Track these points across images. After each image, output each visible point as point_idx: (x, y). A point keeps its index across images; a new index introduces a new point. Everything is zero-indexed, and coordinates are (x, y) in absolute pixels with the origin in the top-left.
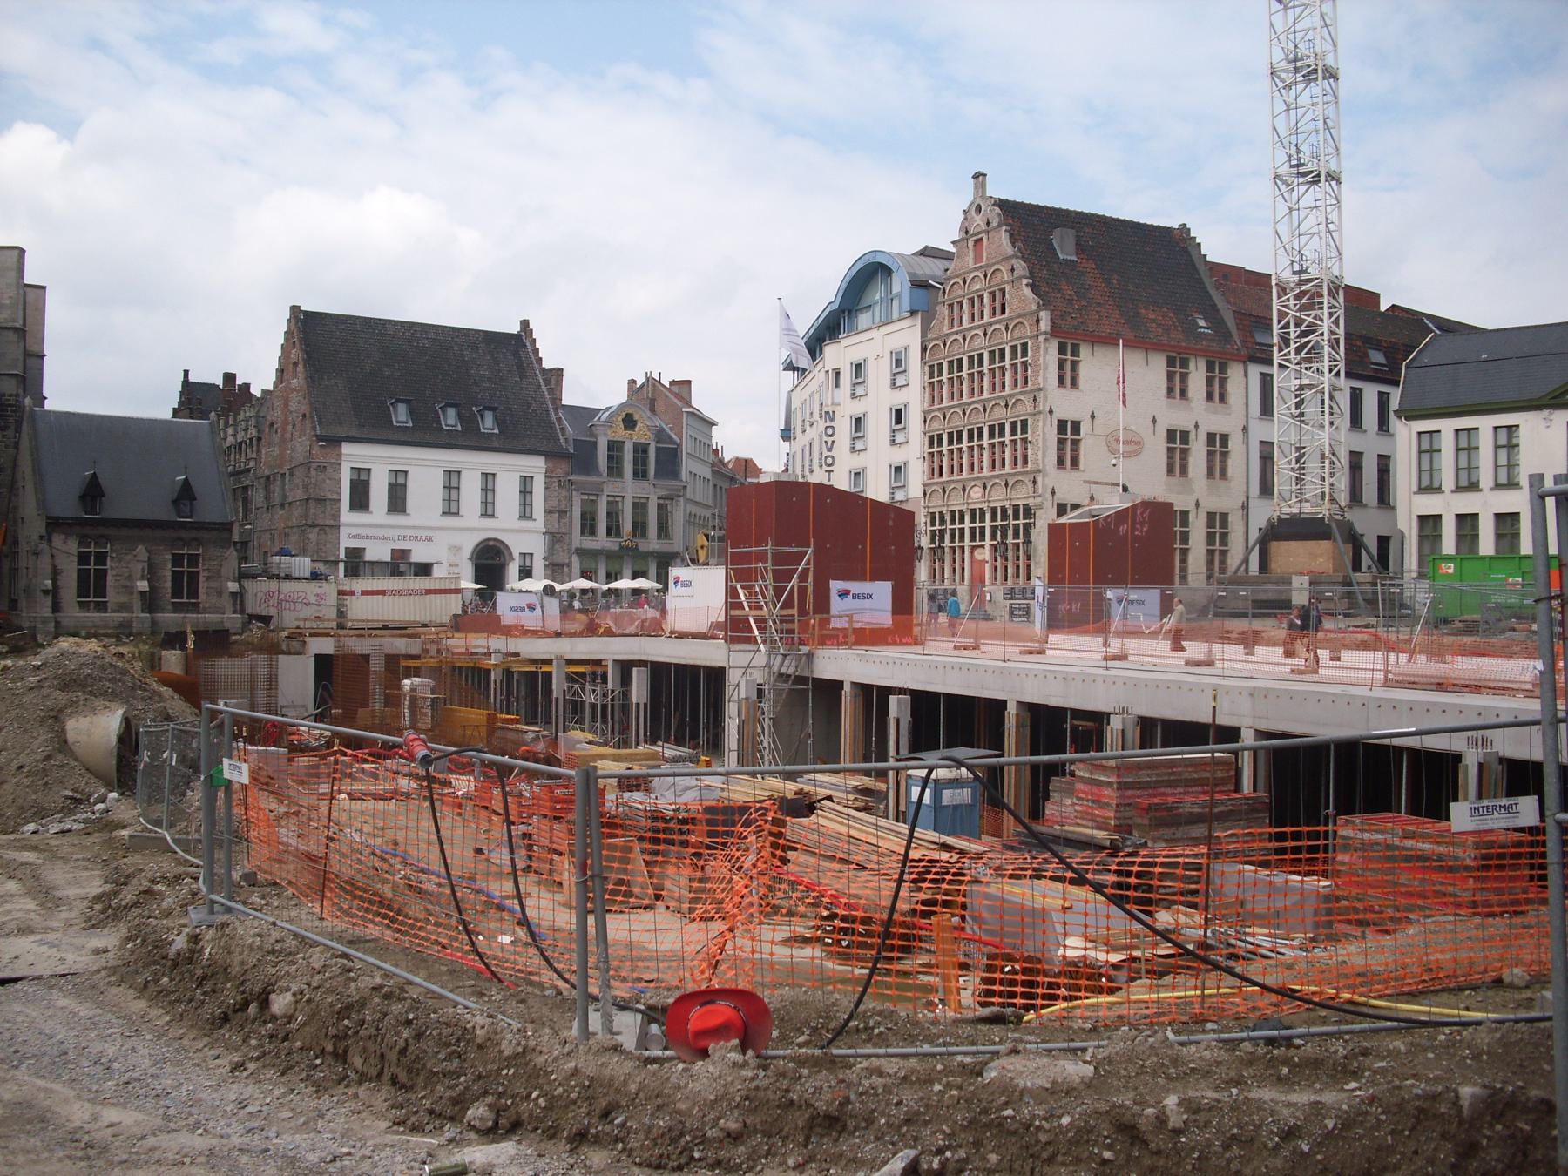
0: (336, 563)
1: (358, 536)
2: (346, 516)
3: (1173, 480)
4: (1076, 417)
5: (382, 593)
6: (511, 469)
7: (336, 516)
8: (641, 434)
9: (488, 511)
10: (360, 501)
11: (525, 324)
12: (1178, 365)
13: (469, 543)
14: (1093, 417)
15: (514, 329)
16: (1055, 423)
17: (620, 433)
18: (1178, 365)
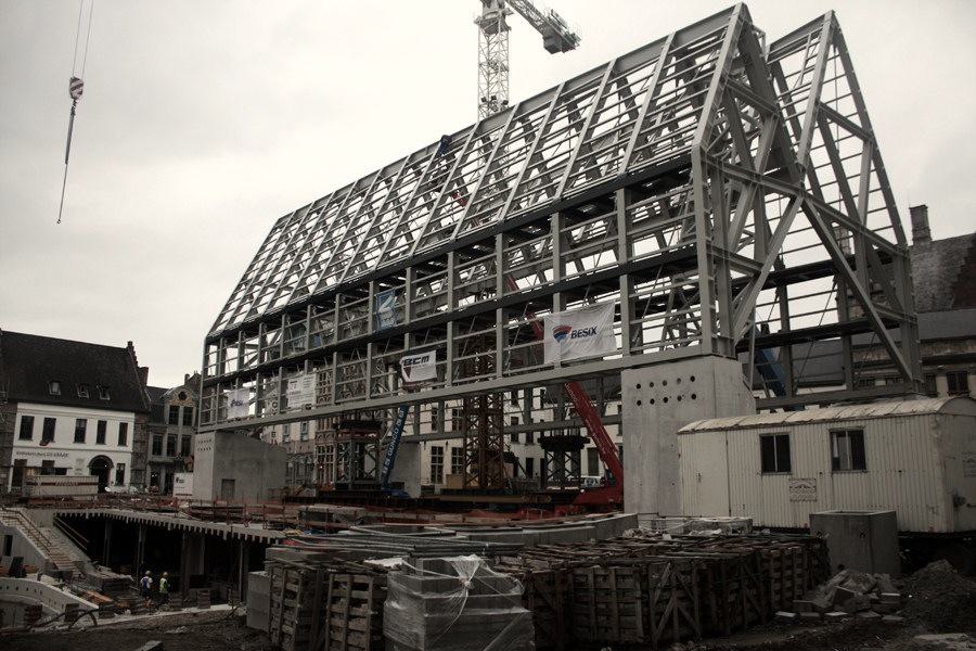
1: (23, 453)
2: (17, 442)
5: (54, 484)
6: (114, 420)
7: (11, 441)
8: (188, 402)
9: (101, 439)
10: (26, 433)
11: (130, 343)
13: (89, 457)
15: (125, 346)
17: (176, 401)
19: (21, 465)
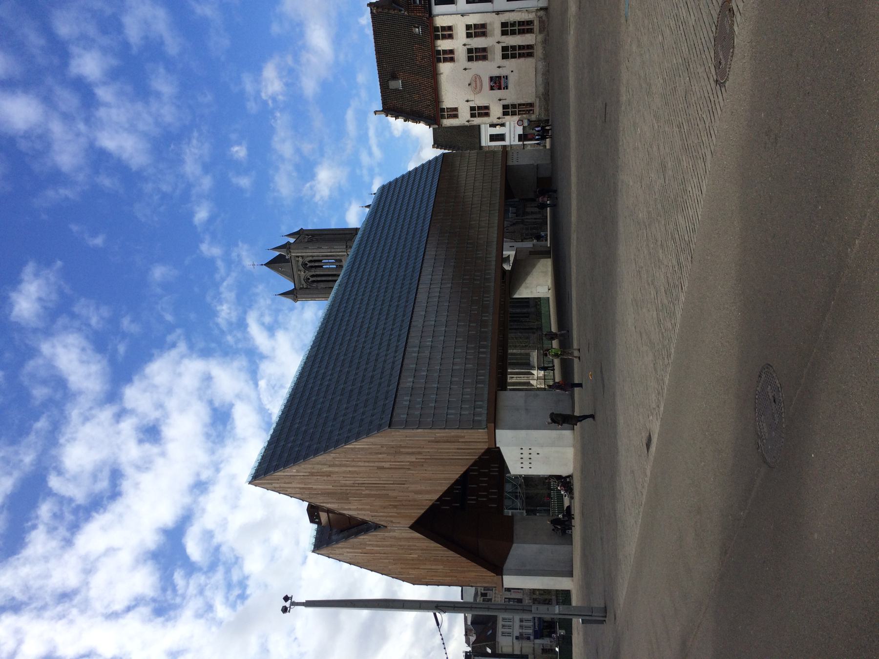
0: (524, 145)
1: (514, 138)
2: (506, 143)
3: (489, 57)
4: (469, 109)
10: (501, 137)
14: (467, 101)
19: (521, 138)
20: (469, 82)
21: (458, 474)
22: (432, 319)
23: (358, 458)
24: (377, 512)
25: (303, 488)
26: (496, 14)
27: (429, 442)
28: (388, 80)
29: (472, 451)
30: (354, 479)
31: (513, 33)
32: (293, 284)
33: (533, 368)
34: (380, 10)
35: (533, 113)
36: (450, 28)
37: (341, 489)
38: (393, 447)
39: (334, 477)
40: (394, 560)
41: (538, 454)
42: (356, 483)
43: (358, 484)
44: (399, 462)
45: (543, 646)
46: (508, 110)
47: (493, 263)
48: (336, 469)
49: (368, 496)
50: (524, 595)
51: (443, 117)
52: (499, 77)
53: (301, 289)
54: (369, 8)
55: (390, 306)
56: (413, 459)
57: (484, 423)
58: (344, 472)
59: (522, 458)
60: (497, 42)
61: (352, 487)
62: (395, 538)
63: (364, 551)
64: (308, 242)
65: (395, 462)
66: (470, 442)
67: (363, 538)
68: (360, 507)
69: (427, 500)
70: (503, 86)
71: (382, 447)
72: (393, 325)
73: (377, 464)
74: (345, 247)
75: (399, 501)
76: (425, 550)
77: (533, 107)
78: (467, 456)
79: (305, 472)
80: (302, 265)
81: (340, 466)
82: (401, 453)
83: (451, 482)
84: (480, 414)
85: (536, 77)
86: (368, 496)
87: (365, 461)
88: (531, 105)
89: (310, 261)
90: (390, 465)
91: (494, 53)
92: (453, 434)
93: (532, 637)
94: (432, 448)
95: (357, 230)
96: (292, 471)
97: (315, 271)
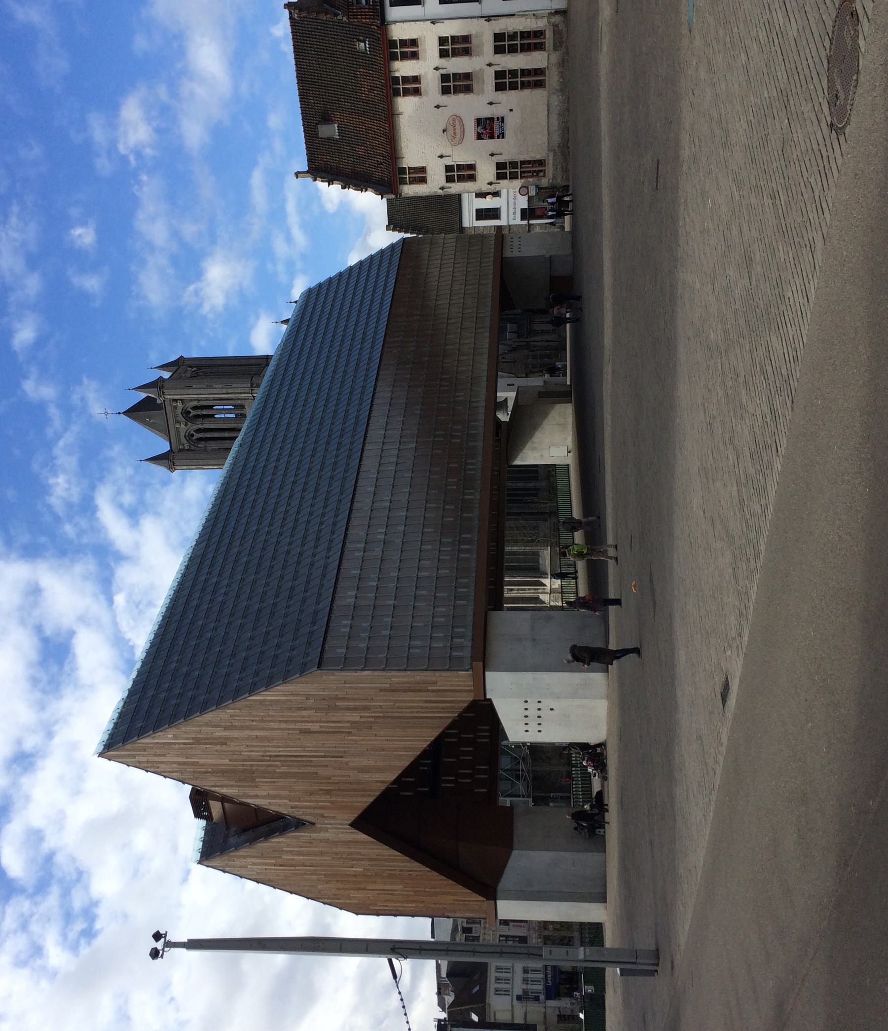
0: (529, 225)
1: (514, 214)
2: (502, 222)
4: (443, 169)
10: (493, 213)
12: (398, 87)
14: (441, 157)
16: (449, 185)
18: (398, 87)
19: (526, 214)
20: (443, 127)
21: (425, 741)
22: (385, 498)
23: (269, 716)
24: (299, 801)
25: (184, 763)
26: (486, 20)
27: (381, 691)
28: (317, 124)
29: (448, 705)
30: (263, 749)
31: (513, 50)
32: (169, 443)
33: (544, 574)
34: (304, 14)
35: (544, 176)
36: (414, 42)
37: (243, 765)
38: (325, 699)
39: (232, 746)
40: (325, 875)
41: (552, 709)
42: (267, 756)
43: (270, 756)
44: (333, 722)
45: (560, 1011)
46: (504, 171)
47: (482, 410)
48: (235, 734)
49: (285, 775)
50: (529, 930)
51: (403, 182)
52: (491, 120)
53: (180, 451)
54: (287, 11)
55: (320, 477)
56: (355, 717)
57: (467, 661)
58: (248, 738)
59: (526, 716)
60: (488, 65)
61: (261, 761)
62: (327, 841)
63: (280, 861)
64: (191, 377)
65: (328, 722)
66: (445, 691)
67: (277, 841)
68: (273, 793)
69: (377, 782)
70: (496, 134)
71: (307, 699)
72: (325, 507)
73: (299, 726)
74: (249, 385)
75: (334, 783)
76: (375, 860)
77: (545, 166)
78: (439, 712)
79: (187, 739)
80: (182, 414)
81: (242, 728)
82: (337, 709)
83: (415, 753)
84: (461, 648)
85: (548, 118)
86: (285, 775)
87: (280, 721)
88: (541, 163)
89: (195, 408)
90: (320, 726)
91: (483, 82)
92: (418, 678)
93: (542, 997)
94: (385, 701)
95: (267, 358)
96: (167, 736)
97: (202, 424)
